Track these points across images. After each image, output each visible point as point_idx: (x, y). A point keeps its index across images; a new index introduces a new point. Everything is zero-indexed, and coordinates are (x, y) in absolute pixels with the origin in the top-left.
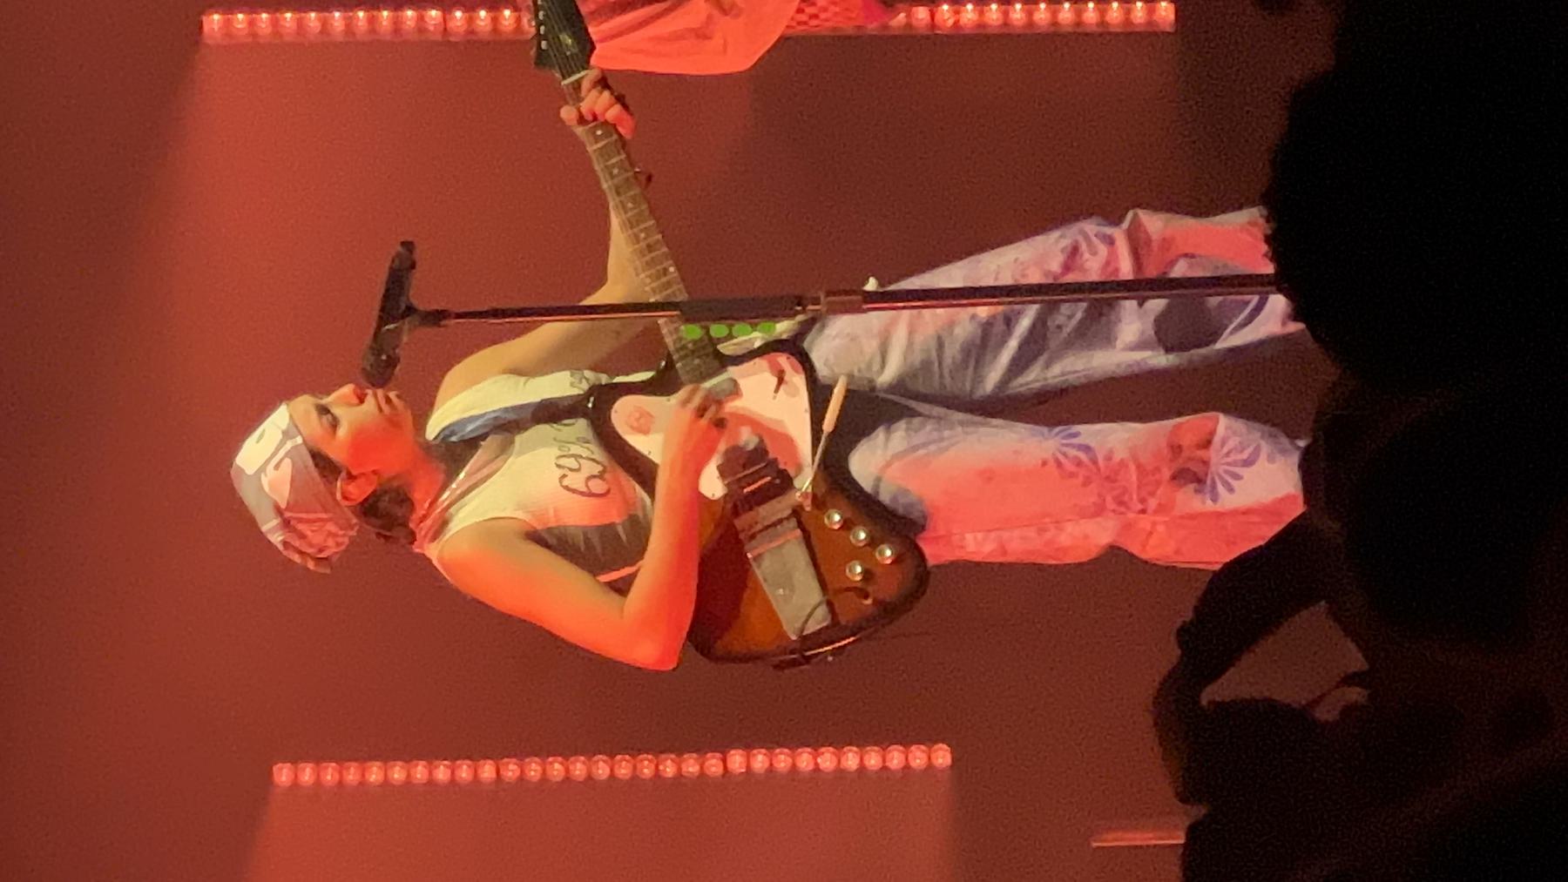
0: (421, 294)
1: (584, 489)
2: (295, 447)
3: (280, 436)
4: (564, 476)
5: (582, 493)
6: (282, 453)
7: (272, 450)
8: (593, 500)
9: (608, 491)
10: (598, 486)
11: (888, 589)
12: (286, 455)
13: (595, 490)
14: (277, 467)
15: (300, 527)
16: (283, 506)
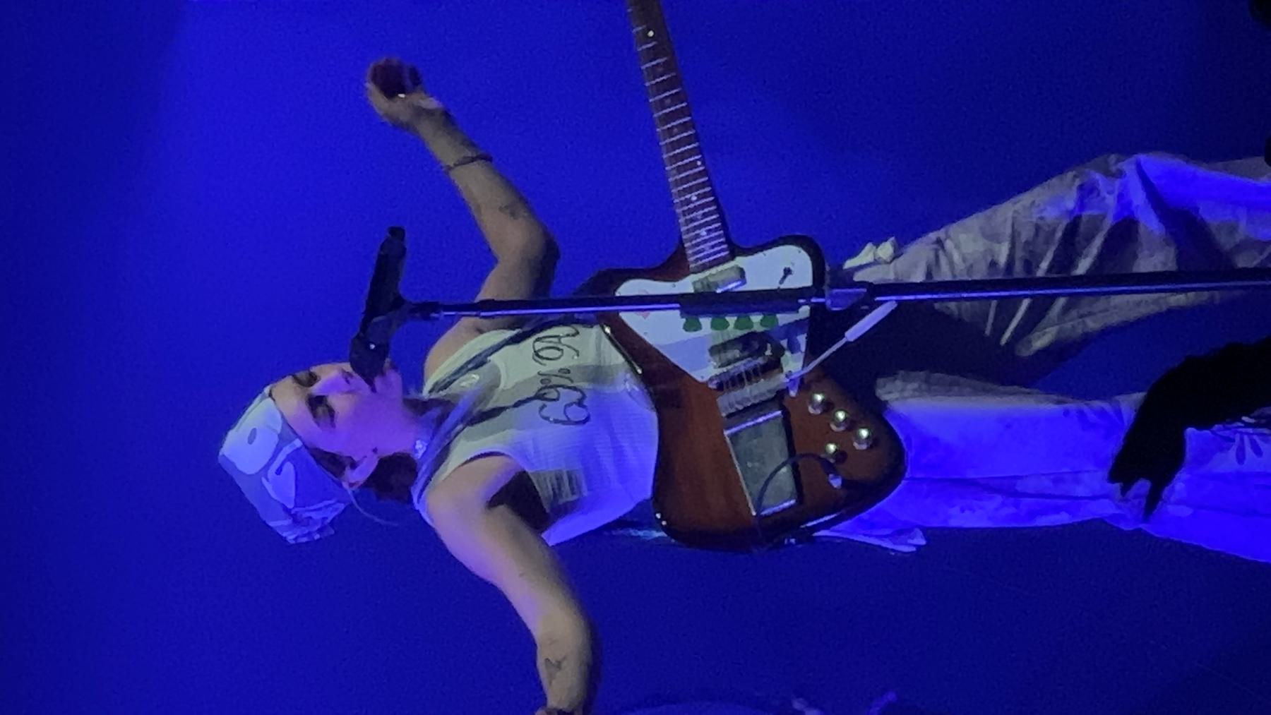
0: (408, 285)
1: (564, 418)
2: (298, 449)
3: (276, 439)
4: (544, 406)
5: (563, 422)
6: (281, 457)
7: (269, 455)
8: (579, 428)
9: (587, 419)
10: (577, 414)
11: (862, 472)
12: (289, 458)
13: (572, 418)
14: (279, 471)
15: (308, 514)
16: (290, 506)
